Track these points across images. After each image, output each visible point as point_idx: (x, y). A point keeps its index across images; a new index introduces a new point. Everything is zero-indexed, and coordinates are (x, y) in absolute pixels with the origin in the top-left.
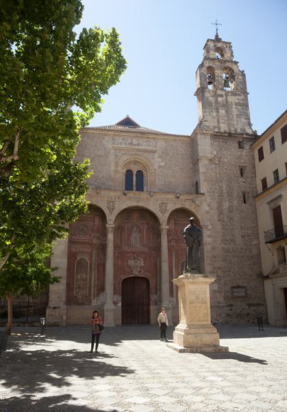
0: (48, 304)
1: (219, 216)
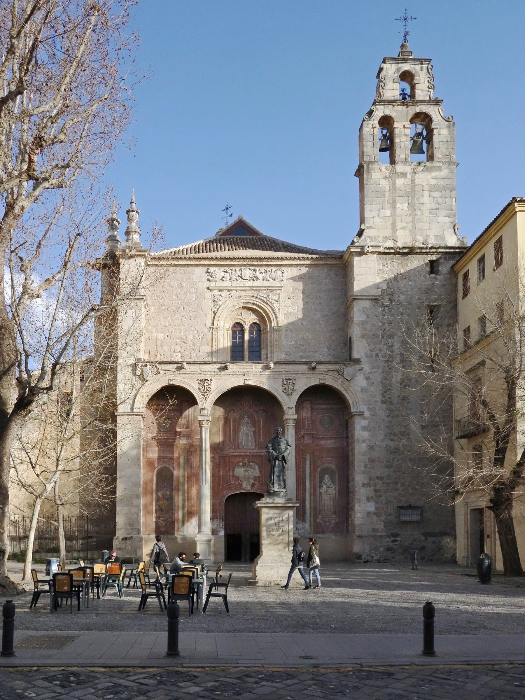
0: (115, 535)
1: (383, 395)
